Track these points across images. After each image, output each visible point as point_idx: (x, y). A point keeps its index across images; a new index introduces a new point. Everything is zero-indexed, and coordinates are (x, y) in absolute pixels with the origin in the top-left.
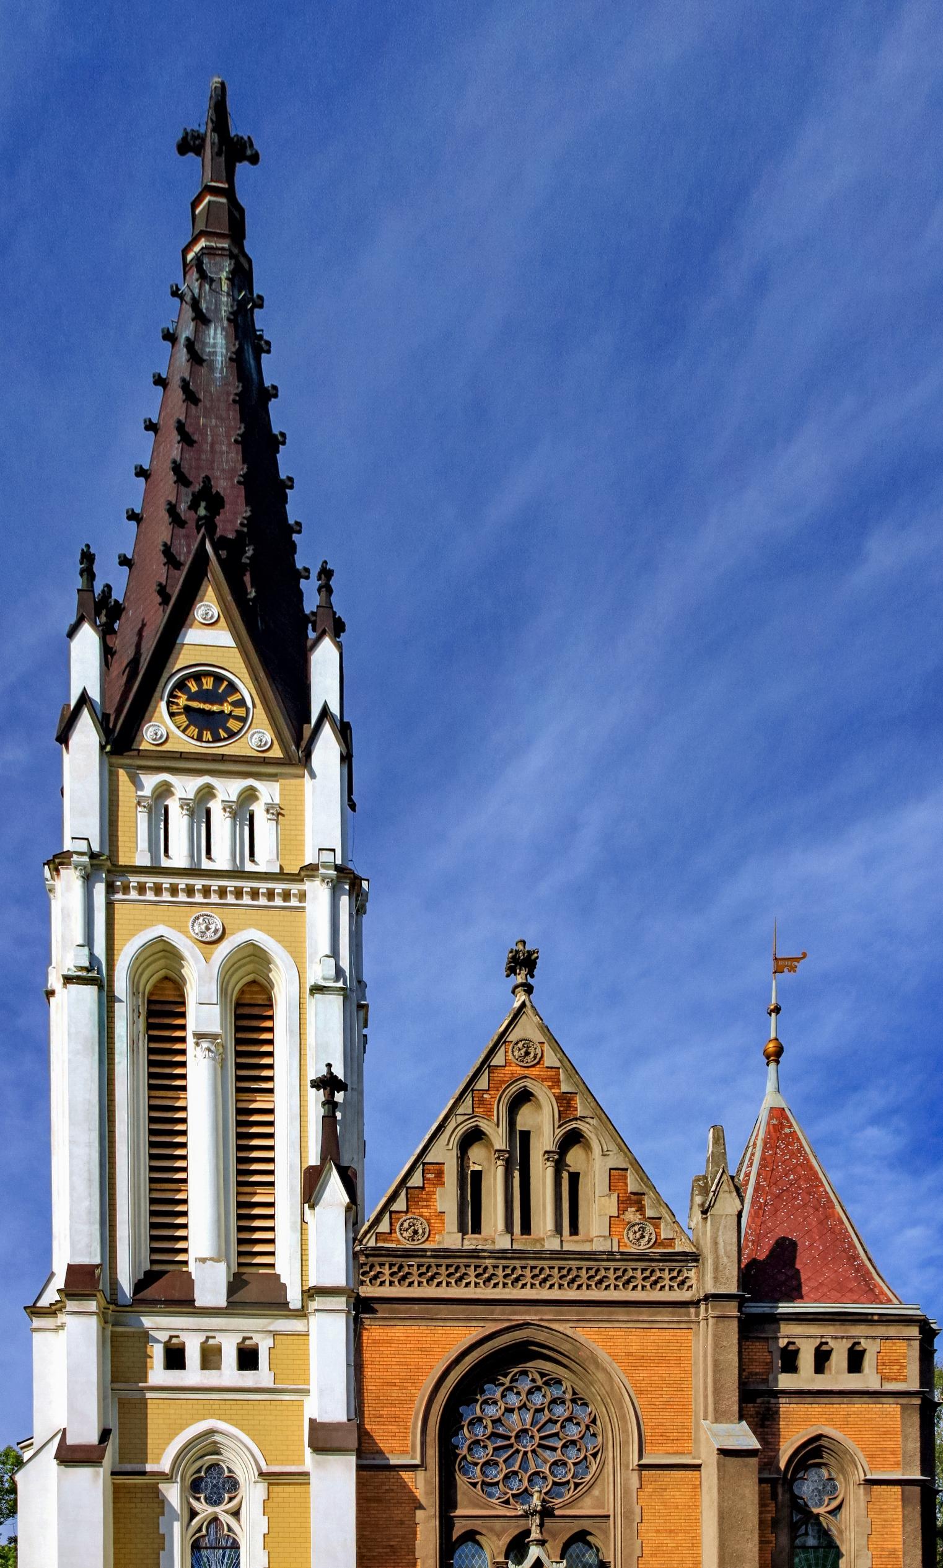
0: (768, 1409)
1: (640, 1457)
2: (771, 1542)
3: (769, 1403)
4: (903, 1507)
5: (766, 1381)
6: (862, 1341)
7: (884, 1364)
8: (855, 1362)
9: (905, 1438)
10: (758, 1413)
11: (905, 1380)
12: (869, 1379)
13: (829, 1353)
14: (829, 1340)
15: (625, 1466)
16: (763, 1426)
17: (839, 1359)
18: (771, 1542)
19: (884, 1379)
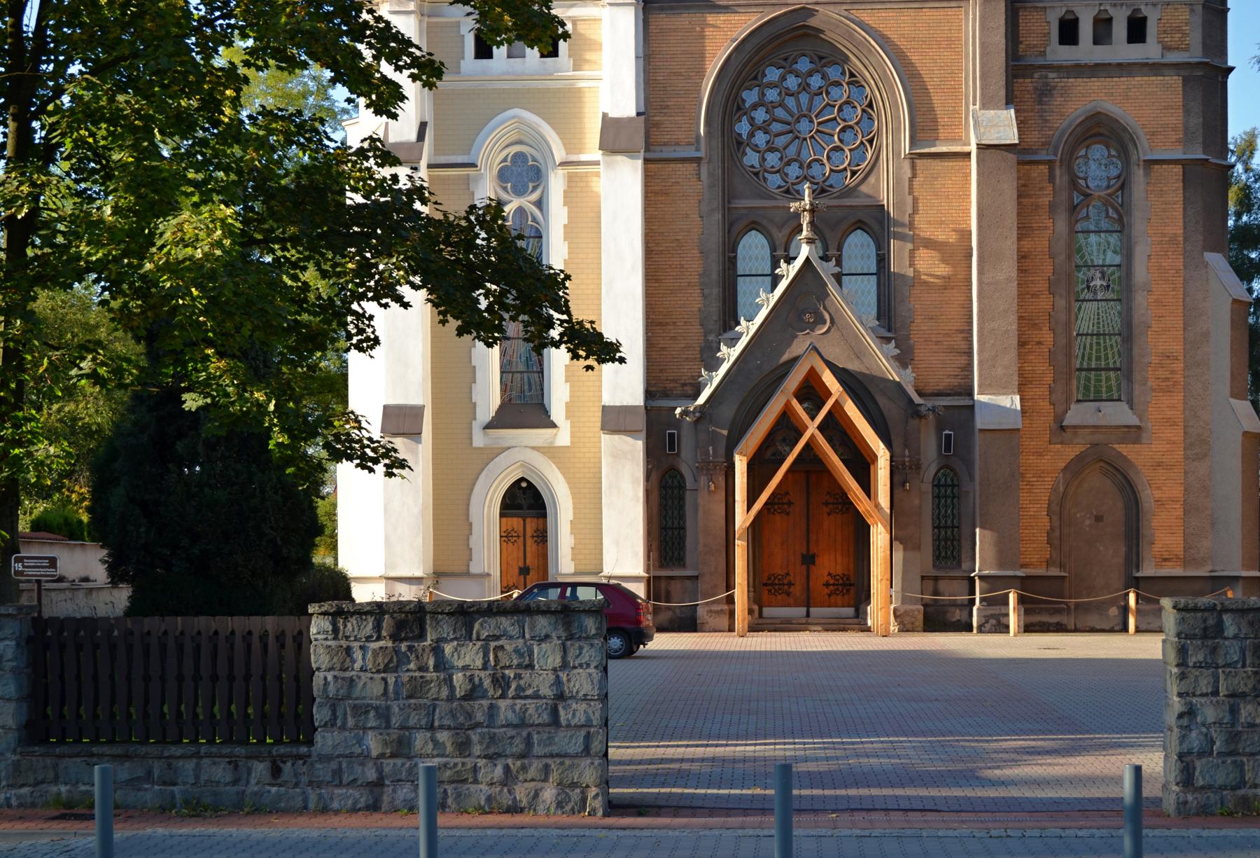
0: (1047, 84)
1: (913, 142)
2: (1046, 228)
3: (1046, 77)
4: (1184, 189)
5: (1043, 54)
6: (1143, 7)
7: (1165, 32)
8: (1137, 31)
9: (1187, 111)
10: (1036, 89)
11: (1187, 49)
12: (1150, 50)
13: (1110, 20)
14: (1108, 8)
15: (896, 153)
16: (1040, 103)
17: (1120, 29)
18: (1046, 228)
19: (1167, 48)
